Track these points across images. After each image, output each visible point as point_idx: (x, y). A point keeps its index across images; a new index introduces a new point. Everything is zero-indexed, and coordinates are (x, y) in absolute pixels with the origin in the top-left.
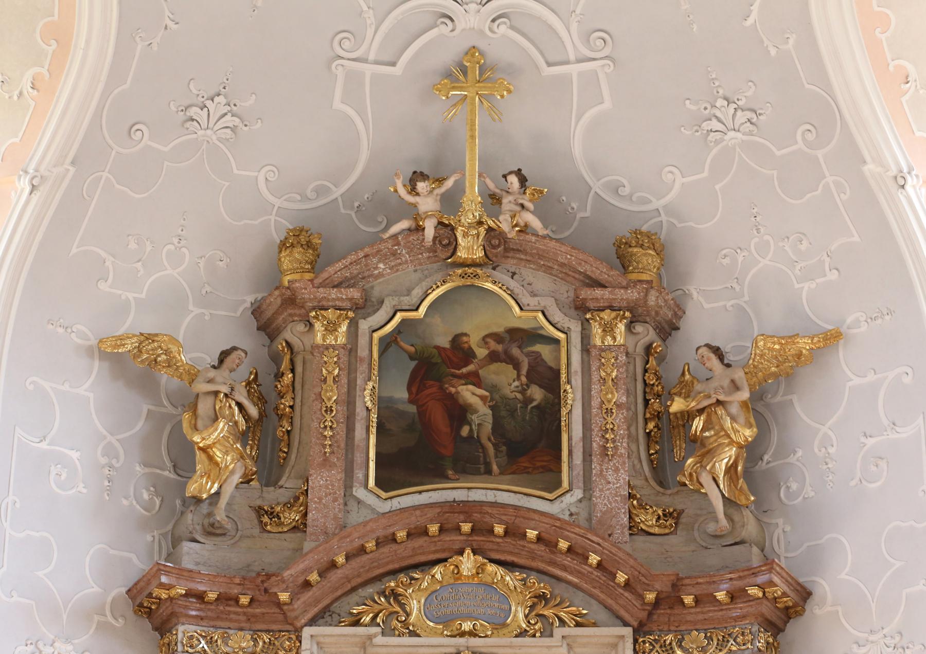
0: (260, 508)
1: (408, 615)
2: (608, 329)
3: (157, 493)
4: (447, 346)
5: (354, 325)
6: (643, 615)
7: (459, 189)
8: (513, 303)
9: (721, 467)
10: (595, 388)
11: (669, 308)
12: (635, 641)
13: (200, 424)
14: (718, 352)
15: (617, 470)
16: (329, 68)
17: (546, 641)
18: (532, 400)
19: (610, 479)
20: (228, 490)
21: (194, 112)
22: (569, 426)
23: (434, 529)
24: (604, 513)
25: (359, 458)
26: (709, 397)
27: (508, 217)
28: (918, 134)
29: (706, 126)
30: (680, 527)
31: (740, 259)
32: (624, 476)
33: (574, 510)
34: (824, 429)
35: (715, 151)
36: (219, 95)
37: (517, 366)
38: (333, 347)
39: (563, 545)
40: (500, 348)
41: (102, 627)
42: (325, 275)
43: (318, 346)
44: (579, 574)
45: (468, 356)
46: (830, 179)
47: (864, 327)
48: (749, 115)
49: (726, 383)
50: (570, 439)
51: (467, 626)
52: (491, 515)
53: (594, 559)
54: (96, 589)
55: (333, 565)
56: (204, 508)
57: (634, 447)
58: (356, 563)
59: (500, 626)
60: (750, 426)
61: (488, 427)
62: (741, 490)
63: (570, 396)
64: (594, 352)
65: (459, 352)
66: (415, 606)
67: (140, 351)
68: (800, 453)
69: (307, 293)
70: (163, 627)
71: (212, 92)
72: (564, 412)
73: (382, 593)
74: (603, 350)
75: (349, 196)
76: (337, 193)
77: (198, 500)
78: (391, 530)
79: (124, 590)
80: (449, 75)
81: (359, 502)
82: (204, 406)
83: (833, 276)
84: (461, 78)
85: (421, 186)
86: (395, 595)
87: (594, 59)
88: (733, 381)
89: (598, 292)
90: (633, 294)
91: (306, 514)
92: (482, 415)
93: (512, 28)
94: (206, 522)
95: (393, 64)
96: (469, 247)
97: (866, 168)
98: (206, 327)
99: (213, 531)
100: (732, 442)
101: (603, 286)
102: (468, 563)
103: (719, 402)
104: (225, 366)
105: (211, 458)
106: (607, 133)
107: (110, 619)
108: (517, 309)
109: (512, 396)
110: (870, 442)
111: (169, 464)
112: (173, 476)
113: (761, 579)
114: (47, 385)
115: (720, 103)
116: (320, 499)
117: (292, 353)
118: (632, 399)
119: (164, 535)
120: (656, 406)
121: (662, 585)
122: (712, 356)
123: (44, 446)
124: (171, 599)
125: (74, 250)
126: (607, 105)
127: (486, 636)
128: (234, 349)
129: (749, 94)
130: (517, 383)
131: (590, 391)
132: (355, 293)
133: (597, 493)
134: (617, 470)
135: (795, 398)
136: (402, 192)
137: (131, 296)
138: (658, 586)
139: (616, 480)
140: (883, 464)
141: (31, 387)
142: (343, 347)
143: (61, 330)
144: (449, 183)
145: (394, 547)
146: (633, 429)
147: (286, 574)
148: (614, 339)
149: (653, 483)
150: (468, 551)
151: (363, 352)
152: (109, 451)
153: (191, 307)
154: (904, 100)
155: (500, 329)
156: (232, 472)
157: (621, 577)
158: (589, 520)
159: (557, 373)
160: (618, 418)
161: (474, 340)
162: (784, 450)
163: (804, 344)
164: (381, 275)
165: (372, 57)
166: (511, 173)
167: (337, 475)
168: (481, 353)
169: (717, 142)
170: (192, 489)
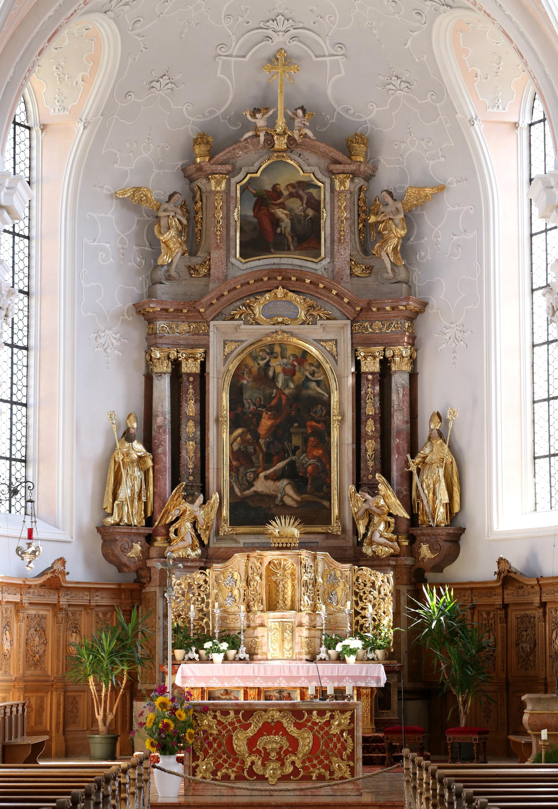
0: (190, 267)
1: (255, 315)
2: (342, 183)
3: (143, 258)
4: (270, 190)
5: (228, 181)
6: (355, 315)
7: (274, 117)
8: (300, 169)
9: (390, 249)
10: (336, 210)
11: (370, 169)
12: (352, 326)
13: (162, 230)
14: (390, 194)
15: (345, 249)
16: (215, 60)
17: (314, 326)
18: (308, 215)
19: (342, 253)
20: (176, 261)
21: (154, 84)
22: (325, 227)
23: (266, 279)
24: (339, 269)
25: (232, 244)
26: (386, 216)
27: (297, 132)
28: (481, 99)
29: (388, 87)
30: (372, 273)
31: (403, 147)
32: (348, 252)
33: (326, 267)
34: (436, 229)
35: (392, 98)
36: (165, 75)
37: (302, 200)
38: (220, 192)
39: (321, 286)
40: (294, 191)
41: (124, 321)
42: (215, 159)
43: (213, 191)
44: (328, 297)
45: (280, 194)
46: (442, 117)
47: (455, 184)
48: (407, 84)
49: (394, 209)
50: (325, 234)
51: (280, 320)
52: (290, 273)
53: (334, 292)
54: (120, 305)
55: (223, 295)
56: (165, 267)
57: (353, 237)
58: (232, 293)
59: (294, 319)
60: (404, 229)
61: (289, 228)
62: (399, 259)
63: (325, 215)
64: (336, 193)
65: (276, 193)
66: (257, 311)
67: (134, 196)
68: (426, 239)
69: (208, 168)
70: (150, 319)
71: (162, 75)
72: (322, 222)
73: (243, 305)
74: (340, 193)
75: (224, 115)
76: (219, 113)
77: (162, 266)
78: (247, 280)
79: (131, 304)
80: (270, 61)
81: (233, 264)
82: (163, 222)
83: (443, 159)
84: (276, 63)
85: (258, 115)
86: (249, 306)
87: (337, 55)
88: (397, 208)
89: (338, 166)
90: (353, 167)
91: (209, 270)
92: (286, 223)
93: (299, 41)
94: (167, 274)
95: (244, 57)
96: (280, 143)
97: (457, 116)
98: (162, 182)
99: (169, 278)
100: (396, 236)
101: (340, 163)
102: (280, 292)
103: (390, 219)
104: (171, 201)
105: (167, 246)
106: (343, 88)
107: (127, 317)
108: (301, 172)
109: (299, 213)
110: (455, 238)
111: (147, 244)
112: (150, 249)
113: (404, 303)
114: (94, 215)
115: (394, 78)
116: (216, 263)
117: (201, 192)
118: (352, 214)
119: (147, 277)
120: (363, 217)
121: (363, 304)
122: (388, 196)
123: (95, 243)
124: (154, 312)
125: (103, 152)
126: (343, 74)
127: (288, 324)
128: (175, 193)
129: (407, 75)
130: (301, 208)
131: (334, 211)
132: (229, 167)
133: (336, 260)
134: (345, 249)
135: (425, 213)
136: (249, 117)
137: (128, 168)
138: (361, 304)
139: (344, 254)
140: (460, 249)
141: (88, 218)
142: (224, 191)
143: (99, 189)
144: (271, 113)
145: (248, 286)
146: (353, 228)
147: (203, 301)
148: (345, 187)
149: (361, 253)
150: (280, 287)
151: (233, 194)
152: (122, 242)
153: (154, 170)
154: (475, 84)
155: (294, 182)
156: (177, 253)
157: (346, 300)
158: (333, 271)
159: (319, 202)
160: (346, 224)
161: (282, 187)
162: (419, 237)
163: (428, 191)
164: (240, 156)
165: (234, 54)
166: (299, 108)
167: (223, 252)
168: (286, 193)
169: (393, 94)
170: (160, 262)
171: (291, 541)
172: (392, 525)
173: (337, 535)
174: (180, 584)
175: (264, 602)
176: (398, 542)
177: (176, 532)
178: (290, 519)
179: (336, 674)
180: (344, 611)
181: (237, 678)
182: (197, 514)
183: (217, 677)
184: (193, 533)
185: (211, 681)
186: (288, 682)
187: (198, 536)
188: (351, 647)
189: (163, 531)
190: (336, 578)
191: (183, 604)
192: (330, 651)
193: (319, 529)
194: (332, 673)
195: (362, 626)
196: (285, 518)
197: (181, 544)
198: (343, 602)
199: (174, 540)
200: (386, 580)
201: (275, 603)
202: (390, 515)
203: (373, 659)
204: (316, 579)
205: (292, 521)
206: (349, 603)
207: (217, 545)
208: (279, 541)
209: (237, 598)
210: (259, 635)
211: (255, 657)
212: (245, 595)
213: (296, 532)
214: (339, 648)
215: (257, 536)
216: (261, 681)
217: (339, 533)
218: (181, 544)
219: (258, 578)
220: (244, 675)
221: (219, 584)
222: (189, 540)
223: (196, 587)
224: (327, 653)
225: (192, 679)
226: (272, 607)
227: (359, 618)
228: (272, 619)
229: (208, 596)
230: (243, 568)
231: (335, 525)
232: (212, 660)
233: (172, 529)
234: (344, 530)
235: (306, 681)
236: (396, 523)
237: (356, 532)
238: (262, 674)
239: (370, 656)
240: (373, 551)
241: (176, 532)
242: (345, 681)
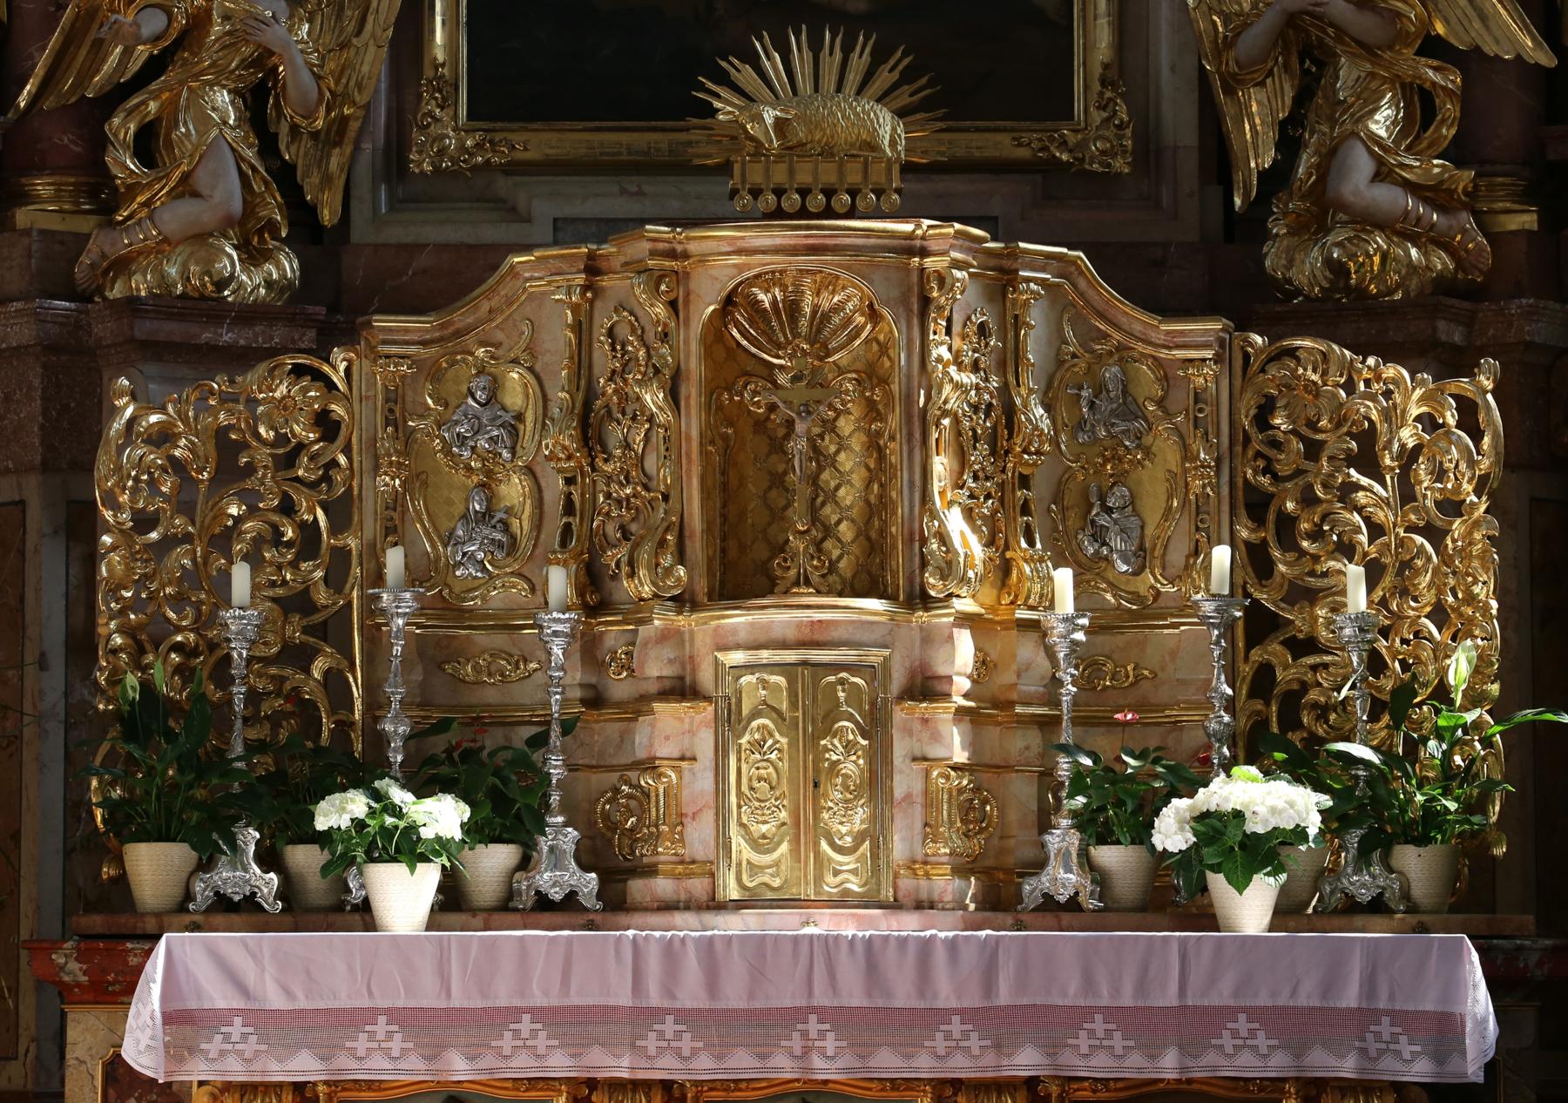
171: (854, 178)
172: (1450, 109)
173: (1110, 178)
174: (162, 438)
175: (697, 548)
176: (1476, 214)
177: (148, 145)
178: (847, 50)
179: (1170, 998)
180: (1187, 608)
181: (526, 1024)
182: (274, 35)
183: (394, 1015)
184: (249, 154)
185: (362, 1044)
186: (863, 1049)
187: (285, 177)
188: (1256, 826)
189: (68, 141)
190: (1129, 409)
191: (182, 558)
192: (1107, 855)
193: (999, 144)
194: (1141, 987)
195: (1292, 701)
196: (816, 46)
197: (178, 216)
198: (1177, 556)
199: (133, 190)
200: (1451, 419)
201: (760, 552)
202: (1433, 47)
203: (1378, 906)
204: (1010, 411)
205: (859, 62)
206: (1221, 556)
207: (397, 233)
208: (779, 175)
209: (522, 526)
210: (664, 750)
211: (638, 888)
212: (569, 508)
213: (886, 126)
214: (1172, 830)
215: (631, 183)
216: (686, 1044)
217: (1120, 165)
218: (178, 216)
219: (653, 398)
220: (575, 1000)
221: (407, 440)
222: (225, 192)
223: (263, 456)
224: (1087, 863)
225: (237, 1028)
226: (741, 576)
227: (1273, 651)
228: (741, 641)
229: (342, 512)
230: (558, 339)
231: (1097, 117)
232: (366, 907)
233: (123, 127)
234: (1149, 150)
235: (974, 1043)
236: (1466, 97)
237: (1219, 157)
238: (691, 994)
239: (1362, 884)
240: (1329, 262)
241: (148, 145)
242: (1227, 1042)
